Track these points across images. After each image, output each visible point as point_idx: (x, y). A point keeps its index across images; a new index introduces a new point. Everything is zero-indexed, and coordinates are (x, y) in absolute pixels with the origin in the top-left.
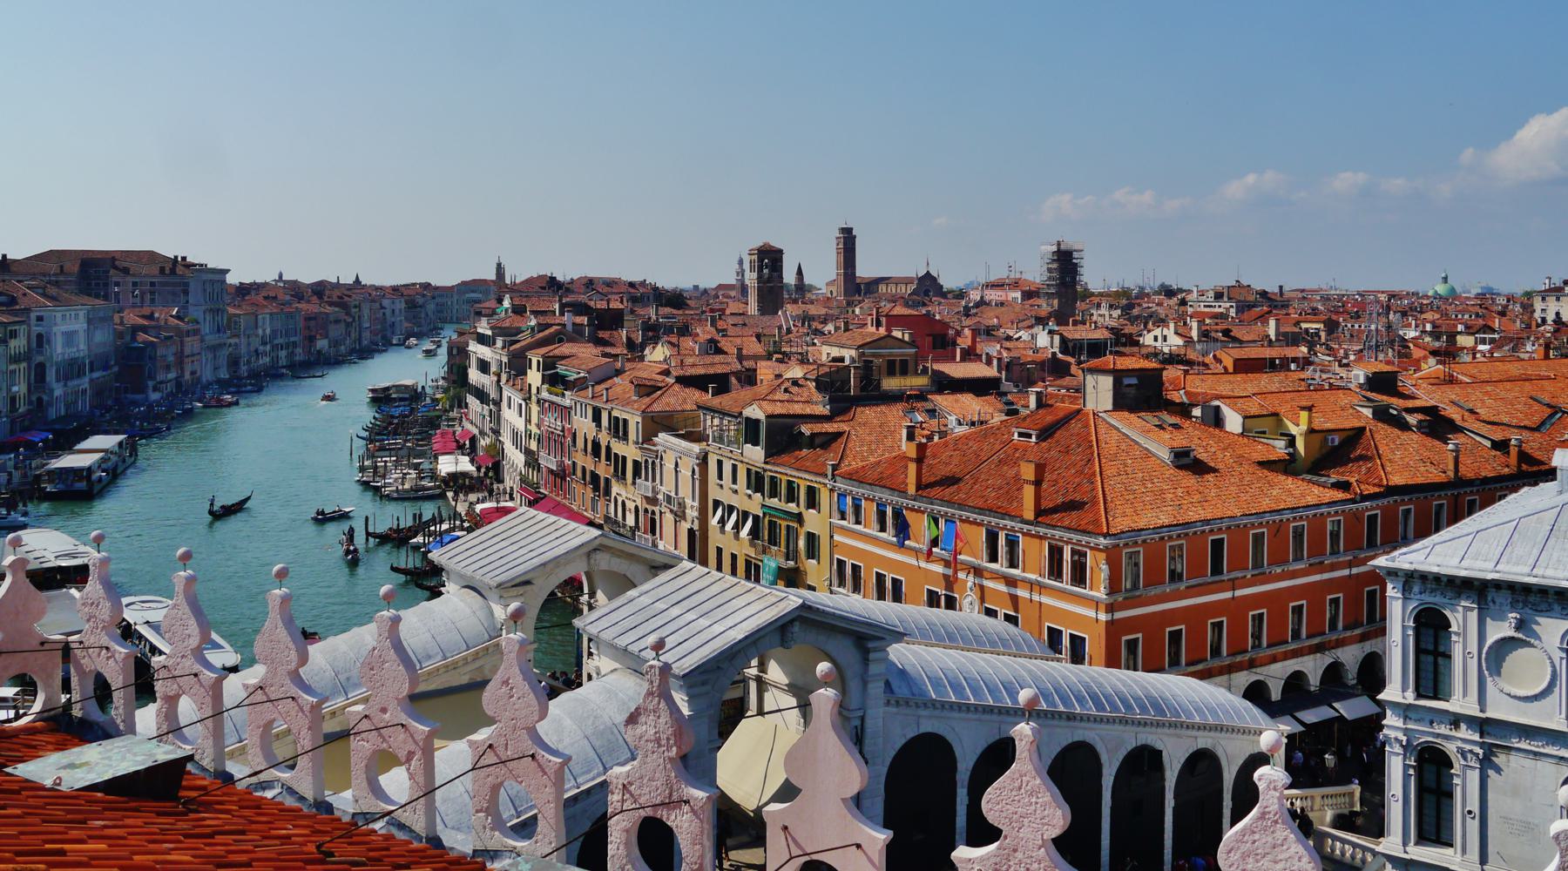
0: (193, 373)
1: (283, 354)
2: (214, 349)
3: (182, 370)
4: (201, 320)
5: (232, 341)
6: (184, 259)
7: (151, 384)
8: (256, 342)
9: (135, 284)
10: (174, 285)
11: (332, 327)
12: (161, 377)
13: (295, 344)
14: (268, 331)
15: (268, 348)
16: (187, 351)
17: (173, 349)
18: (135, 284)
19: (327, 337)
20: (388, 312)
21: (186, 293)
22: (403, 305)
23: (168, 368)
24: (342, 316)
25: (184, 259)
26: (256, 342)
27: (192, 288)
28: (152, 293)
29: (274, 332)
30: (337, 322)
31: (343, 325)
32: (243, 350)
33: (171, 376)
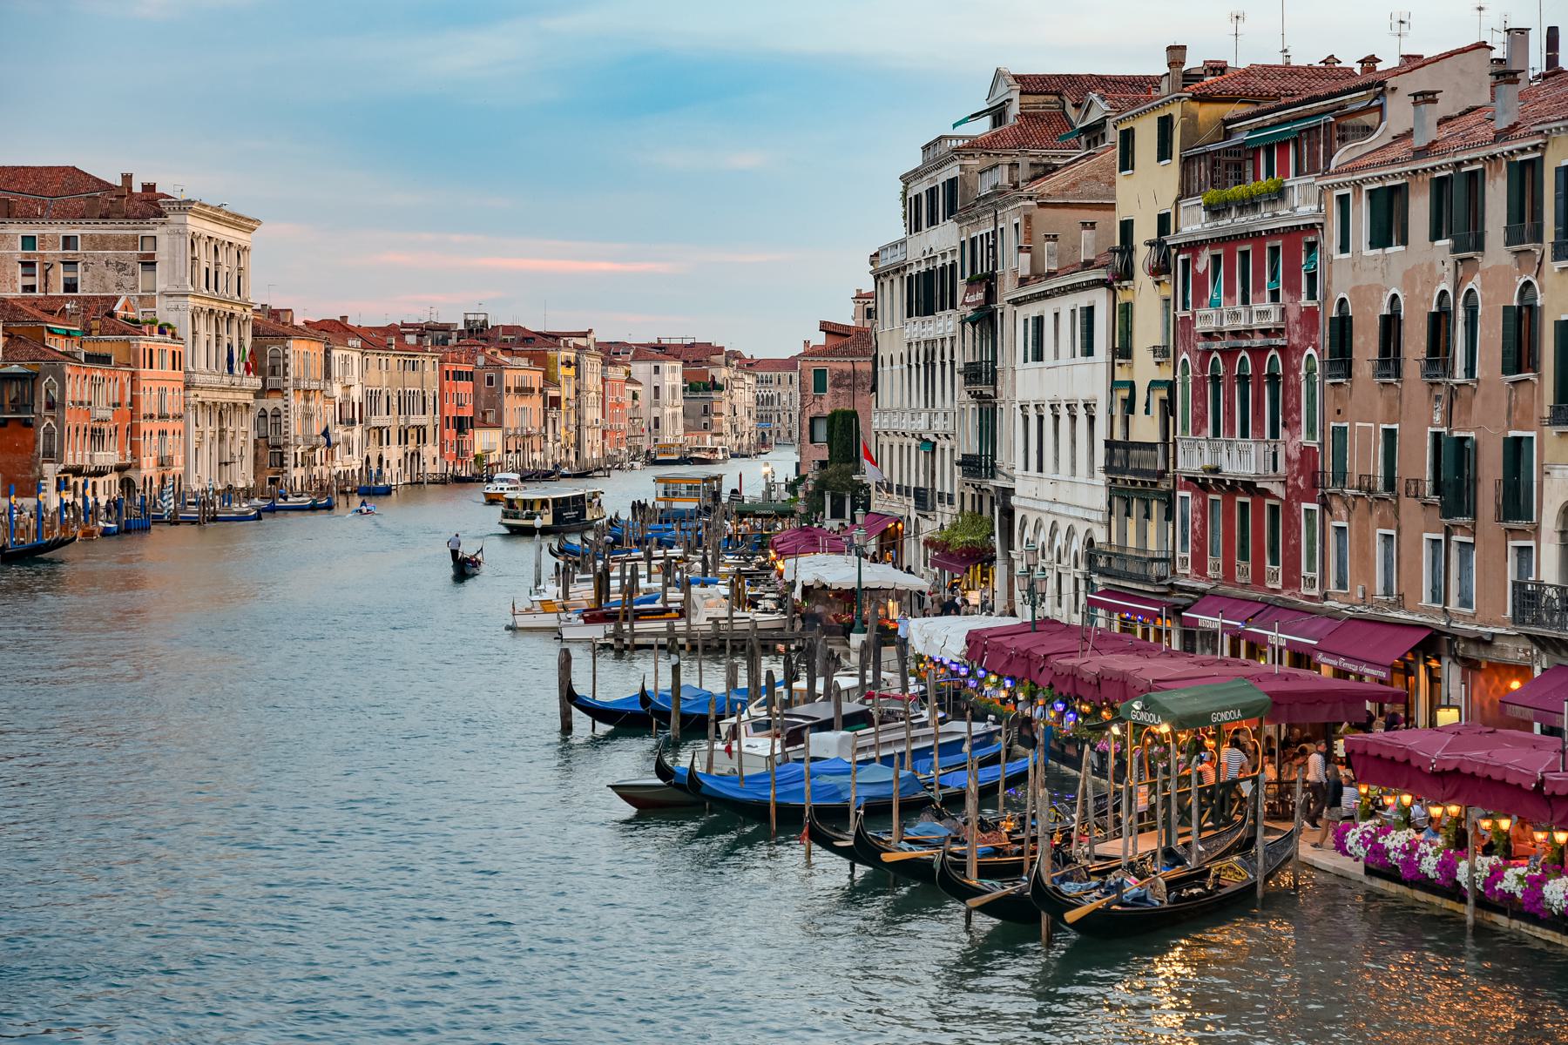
0: (163, 462)
1: (394, 453)
2: (221, 412)
3: (134, 447)
4: (185, 331)
5: (270, 403)
6: (149, 188)
7: (50, 471)
8: (325, 413)
9: (29, 242)
10: (122, 243)
11: (510, 403)
12: (77, 454)
13: (421, 430)
14: (356, 394)
15: (357, 430)
16: (148, 404)
17: (110, 391)
18: (29, 242)
19: (498, 424)
20: (644, 393)
21: (149, 263)
22: (678, 380)
23: (97, 436)
24: (535, 378)
25: (149, 188)
26: (325, 413)
27: (162, 256)
28: (70, 264)
29: (372, 396)
30: (524, 391)
31: (536, 402)
32: (295, 427)
33: (109, 456)
